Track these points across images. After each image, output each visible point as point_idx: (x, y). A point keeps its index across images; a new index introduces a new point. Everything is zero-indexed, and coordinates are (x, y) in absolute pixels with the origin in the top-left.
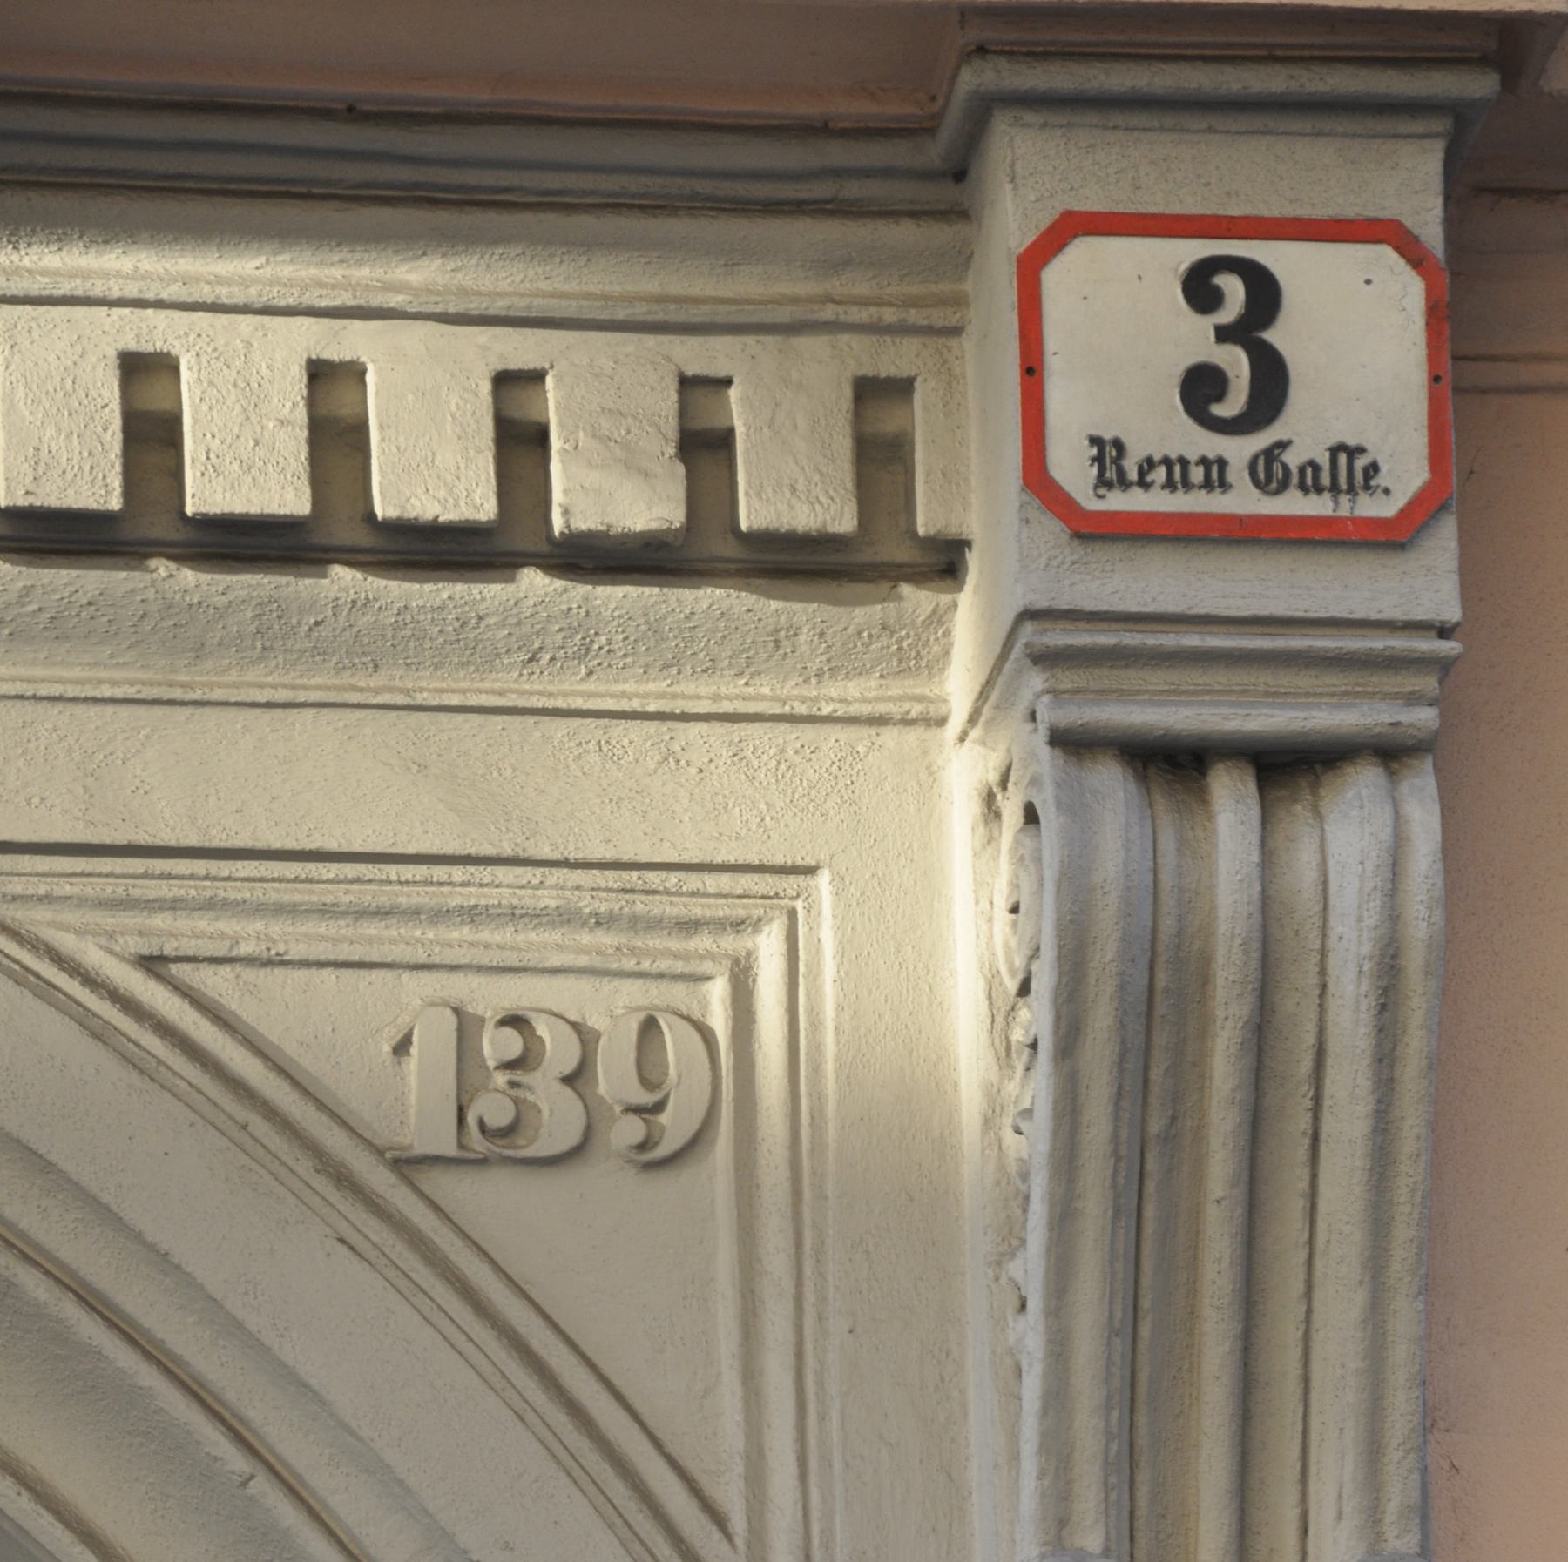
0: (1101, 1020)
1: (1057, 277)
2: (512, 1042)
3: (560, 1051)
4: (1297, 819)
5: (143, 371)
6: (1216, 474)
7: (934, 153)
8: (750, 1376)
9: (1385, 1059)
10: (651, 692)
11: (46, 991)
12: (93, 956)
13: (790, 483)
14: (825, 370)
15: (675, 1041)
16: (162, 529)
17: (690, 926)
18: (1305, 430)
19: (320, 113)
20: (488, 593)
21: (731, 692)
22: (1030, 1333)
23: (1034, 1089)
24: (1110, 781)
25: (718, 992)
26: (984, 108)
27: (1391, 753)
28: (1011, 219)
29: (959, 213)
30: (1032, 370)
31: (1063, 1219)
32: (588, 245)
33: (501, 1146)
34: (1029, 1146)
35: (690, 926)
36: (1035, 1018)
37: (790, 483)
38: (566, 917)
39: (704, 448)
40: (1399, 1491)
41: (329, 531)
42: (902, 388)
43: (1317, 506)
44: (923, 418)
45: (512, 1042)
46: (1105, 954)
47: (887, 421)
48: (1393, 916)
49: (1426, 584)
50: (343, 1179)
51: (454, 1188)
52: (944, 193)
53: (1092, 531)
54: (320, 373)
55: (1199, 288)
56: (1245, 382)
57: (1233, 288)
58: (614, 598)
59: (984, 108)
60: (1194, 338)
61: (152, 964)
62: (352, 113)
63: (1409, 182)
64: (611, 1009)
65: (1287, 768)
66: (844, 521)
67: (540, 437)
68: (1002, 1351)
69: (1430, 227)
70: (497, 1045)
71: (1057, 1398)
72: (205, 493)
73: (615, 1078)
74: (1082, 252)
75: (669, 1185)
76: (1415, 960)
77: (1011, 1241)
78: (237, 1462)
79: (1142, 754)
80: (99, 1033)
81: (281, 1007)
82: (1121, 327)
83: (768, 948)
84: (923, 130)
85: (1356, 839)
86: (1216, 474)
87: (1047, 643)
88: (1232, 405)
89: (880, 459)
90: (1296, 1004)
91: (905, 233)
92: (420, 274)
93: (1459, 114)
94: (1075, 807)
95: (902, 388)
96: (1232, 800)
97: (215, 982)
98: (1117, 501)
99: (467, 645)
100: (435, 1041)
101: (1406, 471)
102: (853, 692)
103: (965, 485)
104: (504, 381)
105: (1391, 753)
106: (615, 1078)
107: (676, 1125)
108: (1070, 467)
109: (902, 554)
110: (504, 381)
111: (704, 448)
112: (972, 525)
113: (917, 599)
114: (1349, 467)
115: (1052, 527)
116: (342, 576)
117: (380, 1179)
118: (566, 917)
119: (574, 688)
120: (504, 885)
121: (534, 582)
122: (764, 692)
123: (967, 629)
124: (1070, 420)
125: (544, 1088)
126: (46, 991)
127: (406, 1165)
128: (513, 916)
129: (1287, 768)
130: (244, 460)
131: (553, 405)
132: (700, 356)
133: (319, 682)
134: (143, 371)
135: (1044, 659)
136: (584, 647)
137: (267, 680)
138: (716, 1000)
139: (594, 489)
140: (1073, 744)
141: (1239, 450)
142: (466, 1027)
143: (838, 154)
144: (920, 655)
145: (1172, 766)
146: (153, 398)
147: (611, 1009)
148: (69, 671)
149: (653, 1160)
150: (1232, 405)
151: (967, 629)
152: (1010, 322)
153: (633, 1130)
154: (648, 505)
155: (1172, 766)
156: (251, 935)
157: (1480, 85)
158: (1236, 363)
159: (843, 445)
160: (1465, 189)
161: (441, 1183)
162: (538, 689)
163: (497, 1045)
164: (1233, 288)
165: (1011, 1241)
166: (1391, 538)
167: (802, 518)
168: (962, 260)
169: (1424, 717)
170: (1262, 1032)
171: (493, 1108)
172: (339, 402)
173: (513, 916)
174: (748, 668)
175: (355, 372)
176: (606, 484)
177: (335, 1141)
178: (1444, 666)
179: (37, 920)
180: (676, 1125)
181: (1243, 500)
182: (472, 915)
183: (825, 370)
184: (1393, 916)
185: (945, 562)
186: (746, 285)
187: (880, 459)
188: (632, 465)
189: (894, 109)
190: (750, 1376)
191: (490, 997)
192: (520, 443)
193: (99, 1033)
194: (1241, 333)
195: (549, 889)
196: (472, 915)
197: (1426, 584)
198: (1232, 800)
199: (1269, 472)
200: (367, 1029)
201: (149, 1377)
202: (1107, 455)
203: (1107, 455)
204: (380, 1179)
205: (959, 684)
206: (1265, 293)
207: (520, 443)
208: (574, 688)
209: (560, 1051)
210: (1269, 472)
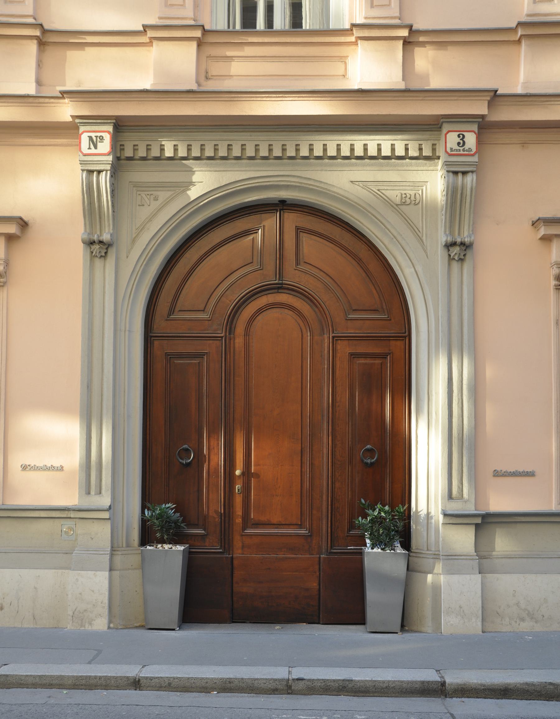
0: (450, 193)
1: (448, 135)
2: (405, 196)
3: (408, 196)
4: (465, 177)
5: (379, 145)
6: (460, 150)
7: (439, 126)
8: (422, 221)
9: (471, 196)
10: (416, 168)
11: (371, 192)
12: (374, 190)
13: (427, 152)
14: (430, 143)
15: (417, 195)
16: (380, 157)
17: (418, 186)
18: (466, 147)
19: (392, 125)
20: (404, 161)
21: (422, 168)
22: (443, 217)
23: (444, 198)
24: (451, 174)
25: (420, 191)
26: (443, 122)
27: (472, 172)
28: (444, 131)
29: (440, 131)
30: (446, 143)
31: (446, 208)
32: (412, 134)
33: (404, 204)
34: (444, 203)
35: (418, 186)
36: (445, 193)
37: (427, 152)
38: (409, 186)
39: (421, 149)
40: (471, 229)
41: (378, 157)
42: (436, 144)
43: (467, 153)
44: (437, 147)
45: (405, 196)
46: (450, 188)
47: (434, 147)
48: (472, 185)
49: (475, 159)
50: (392, 206)
51: (401, 207)
52: (439, 129)
53: (450, 155)
54: (392, 145)
55: (459, 136)
56: (462, 143)
57: (461, 136)
58: (413, 161)
59: (443, 122)
60: (458, 140)
61: (378, 190)
62: (395, 125)
63: (475, 127)
64: (412, 193)
65: (464, 173)
66: (431, 155)
67: (408, 149)
68: (441, 219)
69: (477, 131)
70: (404, 196)
71: (445, 222)
72: (384, 154)
73: (413, 198)
74: (450, 133)
75: (416, 206)
76: (474, 188)
77: (442, 210)
78: (384, 228)
79: (454, 172)
80: (375, 195)
81: (388, 193)
82: (452, 139)
83: (424, 188)
84: (438, 124)
85: (469, 178)
86: (460, 150)
87: (446, 164)
88: (461, 145)
89: (434, 150)
90: (465, 191)
91: (436, 132)
92: (400, 137)
93: (479, 122)
94: (448, 176)
95: (436, 144)
96: (460, 175)
97: (383, 191)
98: (452, 153)
99: (402, 165)
100: (399, 195)
101: (474, 150)
102: (431, 168)
103: (440, 152)
104: (406, 145)
105: (472, 172)
106: (413, 198)
107: (417, 202)
108: (448, 150)
109: (435, 157)
110: (406, 145)
111: (421, 149)
112: (441, 155)
113: (436, 161)
114: (470, 150)
115: (447, 155)
116: (393, 160)
117: (395, 206)
118: (409, 186)
119: (410, 168)
120: (404, 184)
121: (407, 160)
122: (425, 168)
123: (440, 163)
124: (449, 146)
125: (407, 199)
126: (371, 192)
127: (397, 205)
128: (405, 186)
129: (464, 173)
130: (386, 152)
131: (409, 146)
132: (420, 142)
133: (391, 168)
134: (379, 145)
135: (446, 165)
136: (411, 165)
137: (388, 168)
138: (420, 192)
139: (412, 153)
140: (448, 171)
141: (461, 148)
142: (402, 194)
143: (431, 126)
144: (436, 165)
145: (456, 173)
146: (379, 147)
147: (412, 193)
148: (373, 168)
149: (415, 204)
150: (461, 145)
151: (440, 163)
152: (444, 139)
153: (414, 202)
154: (416, 154)
155: (456, 173)
156: (386, 188)
157: (481, 120)
158: (461, 142)
159: (431, 149)
160: (480, 128)
161: (399, 206)
162: (407, 168)
163: (404, 196)
164: (461, 136)
165: (442, 210)
166: (473, 155)
167: (428, 155)
168: (440, 134)
169: (475, 169)
170: (462, 194)
171: (404, 201)
172: (393, 147)
173: (405, 186)
174: (423, 166)
175: (394, 144)
176: (413, 153)
177: (392, 203)
178: (477, 165)
179: (370, 187)
180: (417, 202)
181: (462, 152)
182: (402, 186)
183: (430, 143)
184: (472, 185)
185: (439, 158)
186: (424, 137)
187: (434, 150)
188: (415, 151)
189: (436, 123)
190: (422, 221)
191: (403, 192)
192: (407, 149)
193: (375, 195)
194: (462, 139)
195: (408, 184)
196: (402, 186)
197: (475, 159)
198: (460, 175)
199: (464, 150)
200: (394, 195)
201: (378, 221)
202: (451, 149)
203: (451, 149)
204: (395, 206)
205: (439, 167)
206: (464, 136)
207: (407, 149)
208: (410, 168)
209: (408, 196)
210: (464, 150)
